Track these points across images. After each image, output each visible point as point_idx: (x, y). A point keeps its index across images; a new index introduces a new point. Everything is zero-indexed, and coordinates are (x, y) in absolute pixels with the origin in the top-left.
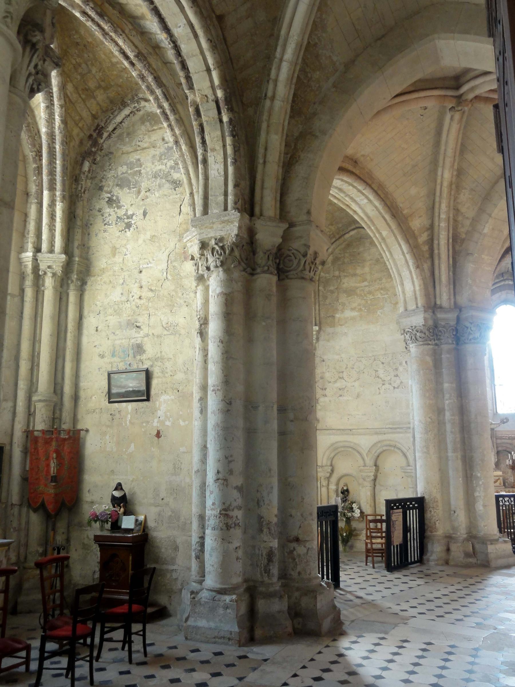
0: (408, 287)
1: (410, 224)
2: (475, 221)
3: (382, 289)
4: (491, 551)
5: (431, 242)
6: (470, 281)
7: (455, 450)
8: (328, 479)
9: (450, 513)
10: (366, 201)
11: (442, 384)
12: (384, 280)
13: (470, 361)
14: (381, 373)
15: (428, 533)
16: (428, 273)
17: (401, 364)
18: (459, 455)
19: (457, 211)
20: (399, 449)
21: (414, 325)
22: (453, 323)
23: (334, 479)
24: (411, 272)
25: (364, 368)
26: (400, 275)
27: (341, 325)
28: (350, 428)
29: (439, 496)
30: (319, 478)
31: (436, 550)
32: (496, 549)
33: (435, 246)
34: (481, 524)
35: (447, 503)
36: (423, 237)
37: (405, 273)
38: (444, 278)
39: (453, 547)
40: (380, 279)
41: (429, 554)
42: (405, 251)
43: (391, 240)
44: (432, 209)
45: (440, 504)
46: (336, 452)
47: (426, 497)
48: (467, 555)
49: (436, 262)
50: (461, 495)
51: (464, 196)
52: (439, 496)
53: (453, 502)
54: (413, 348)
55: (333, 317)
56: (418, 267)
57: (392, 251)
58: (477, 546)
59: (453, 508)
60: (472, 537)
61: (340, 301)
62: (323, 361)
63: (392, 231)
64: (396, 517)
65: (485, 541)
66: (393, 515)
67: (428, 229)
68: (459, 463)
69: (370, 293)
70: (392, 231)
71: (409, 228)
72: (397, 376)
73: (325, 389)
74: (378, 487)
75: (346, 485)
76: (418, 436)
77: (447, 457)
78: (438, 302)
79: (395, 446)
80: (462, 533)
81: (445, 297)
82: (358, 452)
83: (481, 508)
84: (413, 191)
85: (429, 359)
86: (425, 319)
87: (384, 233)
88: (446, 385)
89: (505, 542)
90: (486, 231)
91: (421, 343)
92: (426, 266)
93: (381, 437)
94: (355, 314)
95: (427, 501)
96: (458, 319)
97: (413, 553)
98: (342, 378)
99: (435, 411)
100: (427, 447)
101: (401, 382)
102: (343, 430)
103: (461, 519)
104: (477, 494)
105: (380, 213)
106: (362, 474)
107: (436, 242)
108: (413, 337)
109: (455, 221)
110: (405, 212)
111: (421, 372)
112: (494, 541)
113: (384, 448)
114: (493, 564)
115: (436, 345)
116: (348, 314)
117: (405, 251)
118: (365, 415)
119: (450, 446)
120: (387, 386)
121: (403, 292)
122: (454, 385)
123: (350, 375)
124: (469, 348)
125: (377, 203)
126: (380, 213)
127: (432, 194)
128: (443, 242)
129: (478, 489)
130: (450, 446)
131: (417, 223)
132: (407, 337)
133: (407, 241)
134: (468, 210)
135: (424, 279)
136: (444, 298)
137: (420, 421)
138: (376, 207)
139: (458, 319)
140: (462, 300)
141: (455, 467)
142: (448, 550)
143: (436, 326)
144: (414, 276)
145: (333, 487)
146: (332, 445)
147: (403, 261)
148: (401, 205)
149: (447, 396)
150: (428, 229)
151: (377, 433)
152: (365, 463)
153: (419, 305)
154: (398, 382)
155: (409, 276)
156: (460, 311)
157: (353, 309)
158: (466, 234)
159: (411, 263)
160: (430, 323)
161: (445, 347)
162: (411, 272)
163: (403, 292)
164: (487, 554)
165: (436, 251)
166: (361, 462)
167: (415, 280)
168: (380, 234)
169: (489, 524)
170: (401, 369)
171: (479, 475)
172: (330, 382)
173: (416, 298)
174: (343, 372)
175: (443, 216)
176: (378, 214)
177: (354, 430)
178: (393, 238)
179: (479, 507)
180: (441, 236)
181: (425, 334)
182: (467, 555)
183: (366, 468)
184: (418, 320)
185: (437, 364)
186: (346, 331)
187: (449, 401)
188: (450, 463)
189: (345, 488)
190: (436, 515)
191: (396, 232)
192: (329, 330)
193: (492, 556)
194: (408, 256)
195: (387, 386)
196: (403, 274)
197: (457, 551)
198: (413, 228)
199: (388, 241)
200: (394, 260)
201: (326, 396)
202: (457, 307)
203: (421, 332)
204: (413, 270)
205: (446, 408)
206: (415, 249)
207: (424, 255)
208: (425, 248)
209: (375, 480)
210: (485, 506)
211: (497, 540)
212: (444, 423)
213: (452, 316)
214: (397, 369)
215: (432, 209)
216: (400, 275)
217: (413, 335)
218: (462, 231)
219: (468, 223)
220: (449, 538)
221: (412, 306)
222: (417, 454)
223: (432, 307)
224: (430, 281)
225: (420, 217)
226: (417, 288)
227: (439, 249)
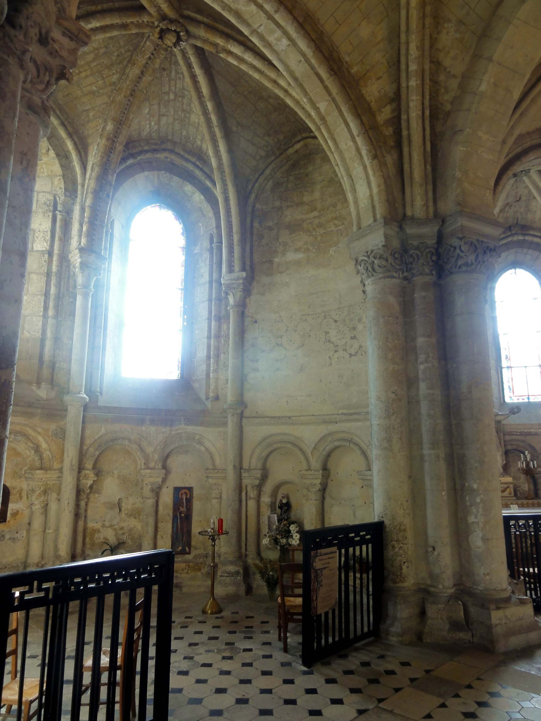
1: (364, 92)
2: (467, 78)
3: (336, 218)
4: (498, 622)
5: (396, 121)
6: (458, 174)
7: (434, 445)
8: (259, 488)
9: (427, 549)
10: (285, 42)
11: (414, 339)
12: (339, 206)
14: (333, 335)
16: (392, 170)
17: (360, 320)
18: (442, 452)
19: (436, 64)
20: (356, 444)
21: (370, 248)
22: (432, 242)
23: (268, 488)
24: (365, 168)
25: (311, 330)
26: (350, 176)
27: (281, 273)
28: (289, 414)
29: (407, 521)
30: (244, 487)
32: (506, 617)
33: (404, 125)
34: (480, 571)
36: (385, 114)
38: (418, 174)
39: (431, 611)
40: (334, 205)
41: (389, 622)
42: (355, 132)
43: (333, 118)
44: (396, 64)
45: (409, 534)
46: (271, 449)
47: (387, 522)
48: (455, 626)
49: (406, 150)
50: (445, 520)
51: (448, 37)
52: (407, 521)
53: (430, 532)
55: (271, 262)
56: (375, 157)
57: (336, 137)
58: (473, 610)
59: (431, 541)
60: (465, 591)
61: (280, 240)
62: (256, 322)
63: (334, 100)
64: (324, 562)
66: (317, 559)
67: (392, 101)
68: (443, 465)
69: (320, 225)
70: (334, 100)
71: (361, 98)
72: (354, 338)
73: (257, 361)
74: (328, 501)
75: (288, 497)
77: (422, 456)
78: (409, 213)
79: (350, 441)
80: (446, 585)
81: (419, 202)
82: (301, 450)
83: (479, 543)
84: (365, 31)
86: (386, 236)
87: (322, 106)
88: (421, 341)
89: (522, 602)
90: (483, 88)
91: (381, 275)
92: (390, 159)
93: (332, 428)
94: (300, 256)
95: (388, 529)
98: (281, 345)
99: (402, 382)
100: (389, 440)
101: (361, 347)
102: (279, 417)
103: (446, 560)
104: (471, 519)
105: (313, 68)
106: (305, 481)
107: (404, 117)
108: (370, 269)
109: (434, 82)
110: (354, 70)
111: (381, 320)
113: (337, 444)
114: (501, 647)
115: (405, 278)
116: (291, 256)
117: (355, 132)
118: (310, 396)
119: (426, 438)
120: (341, 353)
121: (356, 202)
122: (434, 340)
123: (291, 341)
125: (302, 44)
126: (313, 68)
127: (394, 35)
128: (414, 113)
129: (474, 510)
130: (426, 438)
131: (374, 90)
133: (358, 116)
134: (454, 62)
135: (386, 179)
137: (378, 398)
138: (304, 55)
139: (440, 237)
140: (447, 206)
141: (434, 471)
142: (423, 613)
143: (404, 249)
144: (370, 172)
145: (266, 499)
146: (265, 438)
147: (354, 152)
148: (347, 59)
149: (422, 357)
150: (392, 101)
151: (325, 422)
152: (309, 466)
153: (378, 216)
154: (356, 346)
155: (362, 175)
156: (443, 221)
157: (297, 250)
158: (452, 103)
159: (364, 152)
160: (396, 243)
161: (419, 280)
162: (365, 168)
163: (356, 202)
164: (490, 628)
165: (405, 133)
166: (304, 465)
167: (372, 178)
168: (317, 109)
169: (494, 571)
170: (360, 327)
171: (475, 486)
172: (264, 351)
173: (373, 207)
174: (281, 337)
175: (413, 67)
176: (308, 67)
177: (294, 418)
178: (336, 113)
179: (476, 541)
180: (412, 104)
181: (387, 260)
182: (455, 626)
183: (310, 472)
184: (376, 240)
185: (407, 307)
186: (287, 280)
187: (425, 366)
188: (427, 466)
189: (284, 501)
190: (404, 554)
191: (339, 99)
192: (265, 280)
193: (499, 630)
194: (359, 140)
195: (341, 353)
196: (354, 173)
197: (438, 618)
198: (368, 98)
199: (329, 119)
200: (341, 153)
201: (258, 370)
203: (381, 257)
204: (367, 162)
205: (421, 376)
206: (370, 129)
207: (386, 140)
208: (389, 131)
209: (324, 489)
210: (485, 540)
211: (507, 600)
212: (418, 402)
213: (429, 231)
214: (354, 328)
215: (396, 64)
216: (350, 176)
217: (369, 264)
218: (446, 98)
219: (454, 84)
224: (396, 182)
225: (379, 79)
226: (375, 190)
227: (408, 129)
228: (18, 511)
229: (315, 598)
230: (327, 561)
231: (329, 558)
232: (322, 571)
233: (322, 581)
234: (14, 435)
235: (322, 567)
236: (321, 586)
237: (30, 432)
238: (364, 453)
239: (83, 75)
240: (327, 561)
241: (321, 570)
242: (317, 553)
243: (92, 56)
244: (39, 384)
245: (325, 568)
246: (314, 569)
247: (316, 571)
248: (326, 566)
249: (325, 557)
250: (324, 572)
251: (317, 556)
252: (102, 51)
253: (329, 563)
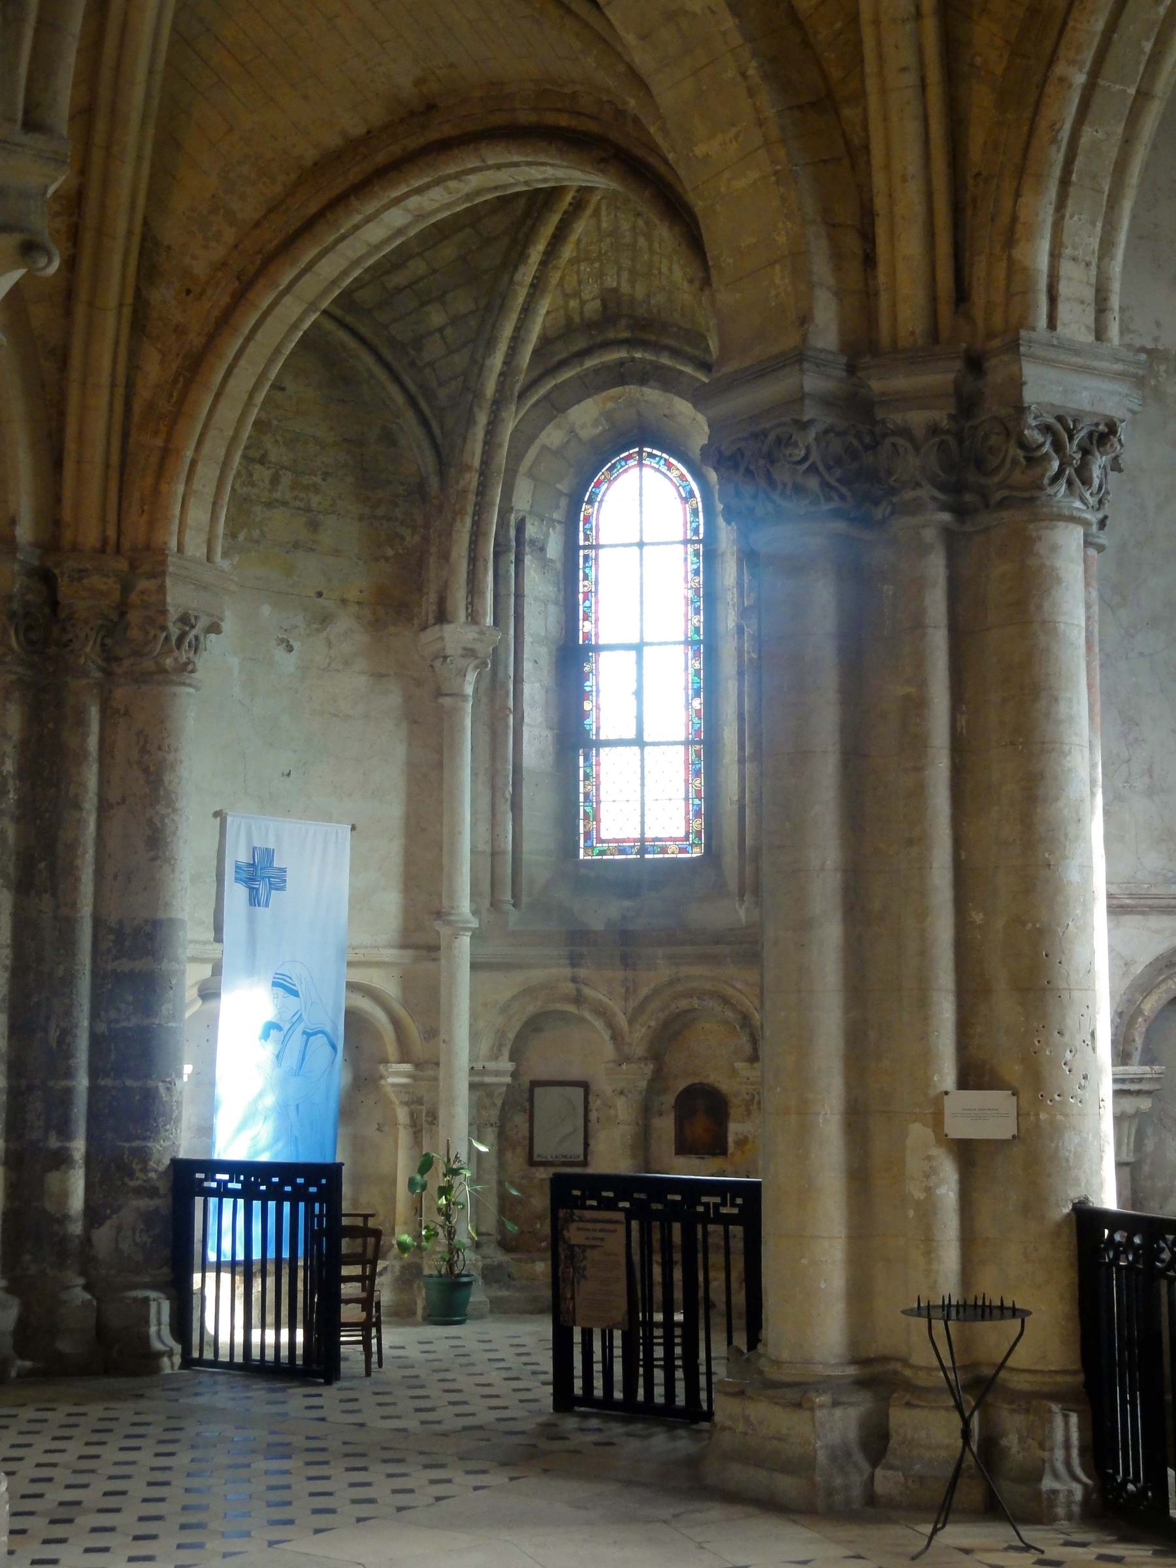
4: (729, 1423)
32: (747, 1419)
66: (573, 1227)
228: (746, 1138)
229: (569, 1296)
230: (599, 1235)
231: (601, 1230)
232: (584, 1251)
233: (584, 1269)
234: (699, 998)
235: (588, 1243)
236: (584, 1277)
237: (730, 991)
239: (665, 270)
240: (599, 1235)
241: (584, 1248)
242: (572, 1214)
243: (642, 242)
244: (741, 895)
245: (593, 1247)
246: (565, 1242)
247: (571, 1247)
248: (598, 1243)
249: (589, 1226)
250: (589, 1253)
251: (573, 1221)
252: (640, 222)
253: (602, 1239)
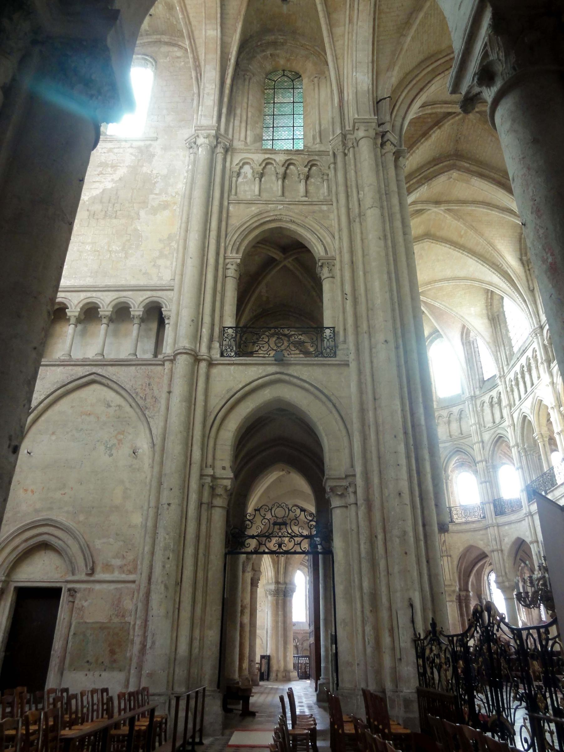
0: (270, 574)
9: (278, 661)
13: (288, 603)
15: (271, 669)
22: (283, 589)
31: (273, 675)
35: (278, 658)
37: (269, 568)
38: (282, 572)
39: (279, 675)
48: (283, 677)
52: (275, 655)
54: (270, 597)
65: (289, 672)
76: (269, 632)
80: (282, 668)
85: (275, 602)
92: (276, 566)
96: (285, 588)
97: (265, 677)
99: (276, 622)
112: (292, 672)
124: (288, 598)
132: (268, 593)
136: (281, 580)
139: (285, 588)
140: (287, 581)
142: (277, 675)
143: (278, 589)
161: (281, 598)
169: (291, 666)
179: (288, 659)
182: (283, 677)
184: (273, 587)
185: (277, 604)
187: (280, 619)
190: (274, 662)
193: (291, 677)
197: (280, 675)
202: (285, 583)
213: (284, 586)
220: (278, 671)
221: (270, 581)
222: (268, 639)
223: (277, 582)
224: (277, 572)
238: (261, 639)
